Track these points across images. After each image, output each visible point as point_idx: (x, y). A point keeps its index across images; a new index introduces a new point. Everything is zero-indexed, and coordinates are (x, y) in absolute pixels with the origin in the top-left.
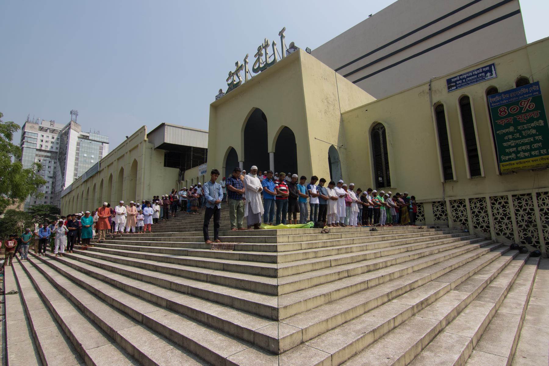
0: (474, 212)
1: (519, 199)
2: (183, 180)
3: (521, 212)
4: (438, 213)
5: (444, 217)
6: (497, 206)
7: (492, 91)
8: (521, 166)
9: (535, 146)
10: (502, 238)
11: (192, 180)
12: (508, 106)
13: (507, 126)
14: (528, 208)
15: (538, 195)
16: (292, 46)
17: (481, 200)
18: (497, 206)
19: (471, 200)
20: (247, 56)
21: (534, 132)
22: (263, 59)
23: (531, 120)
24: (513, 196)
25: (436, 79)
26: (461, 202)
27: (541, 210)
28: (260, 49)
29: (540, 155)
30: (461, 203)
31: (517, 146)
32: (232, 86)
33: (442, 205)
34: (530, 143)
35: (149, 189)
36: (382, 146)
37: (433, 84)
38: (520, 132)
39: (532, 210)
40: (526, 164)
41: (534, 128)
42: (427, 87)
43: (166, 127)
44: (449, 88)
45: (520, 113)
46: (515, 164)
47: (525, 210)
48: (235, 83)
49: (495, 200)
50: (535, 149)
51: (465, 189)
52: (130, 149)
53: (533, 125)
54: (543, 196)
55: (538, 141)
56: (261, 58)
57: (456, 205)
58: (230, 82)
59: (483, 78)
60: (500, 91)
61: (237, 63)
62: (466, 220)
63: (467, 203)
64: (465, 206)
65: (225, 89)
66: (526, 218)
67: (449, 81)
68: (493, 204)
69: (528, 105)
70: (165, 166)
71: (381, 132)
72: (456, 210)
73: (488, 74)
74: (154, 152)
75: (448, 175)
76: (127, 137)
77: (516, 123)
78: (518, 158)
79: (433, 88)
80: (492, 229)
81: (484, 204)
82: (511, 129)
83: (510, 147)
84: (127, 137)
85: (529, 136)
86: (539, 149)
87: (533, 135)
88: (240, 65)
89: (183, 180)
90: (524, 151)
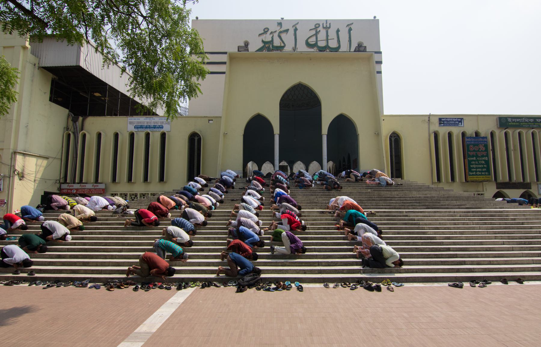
7: (463, 134)
8: (477, 179)
9: (484, 170)
11: (116, 136)
12: (474, 145)
13: (473, 156)
21: (483, 162)
23: (483, 156)
25: (433, 115)
29: (485, 175)
31: (476, 168)
34: (482, 168)
35: (27, 134)
36: (393, 150)
38: (478, 161)
40: (480, 179)
41: (484, 160)
42: (427, 119)
44: (440, 124)
45: (478, 151)
46: (475, 178)
50: (484, 172)
53: (483, 159)
55: (484, 168)
59: (457, 125)
67: (440, 120)
69: (482, 148)
70: (51, 100)
74: (37, 72)
75: (439, 179)
77: (477, 156)
78: (476, 175)
79: (431, 121)
82: (474, 158)
83: (473, 168)
85: (482, 164)
86: (485, 172)
87: (483, 164)
90: (479, 172)
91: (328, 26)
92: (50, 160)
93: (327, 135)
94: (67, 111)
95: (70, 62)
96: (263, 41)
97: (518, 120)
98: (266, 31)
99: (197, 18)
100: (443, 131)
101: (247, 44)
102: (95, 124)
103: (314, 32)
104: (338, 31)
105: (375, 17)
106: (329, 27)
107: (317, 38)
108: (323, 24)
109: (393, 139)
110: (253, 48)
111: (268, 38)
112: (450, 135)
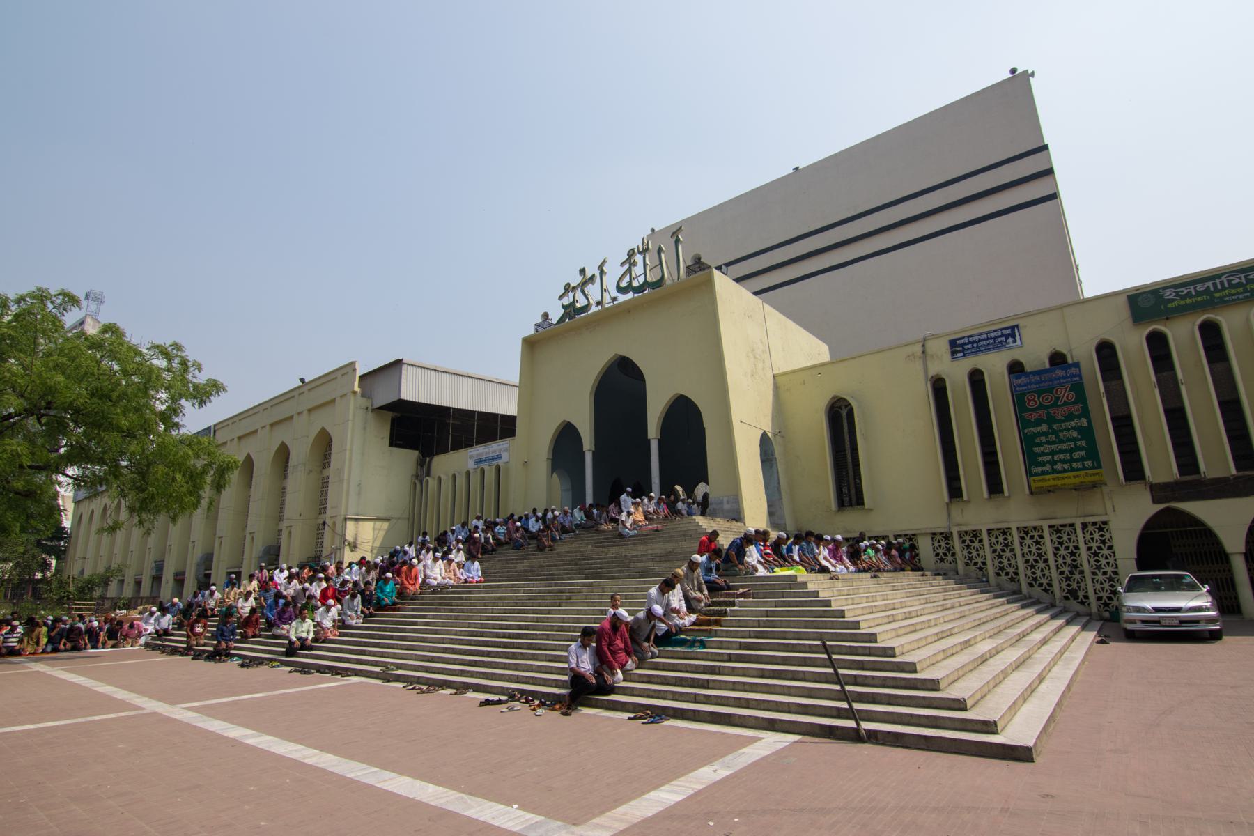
0: (994, 551)
1: (1058, 531)
2: (428, 475)
3: (1062, 552)
4: (941, 552)
5: (949, 558)
6: (1028, 541)
7: (1015, 368)
8: (1059, 483)
9: (1077, 455)
10: (1037, 591)
11: (454, 477)
12: (1039, 393)
13: (1038, 423)
14: (1071, 545)
15: (1084, 526)
17: (1005, 532)
18: (1028, 541)
19: (989, 531)
20: (604, 261)
21: (1075, 434)
22: (638, 270)
23: (1070, 417)
24: (1050, 527)
25: (933, 337)
26: (976, 534)
27: (1089, 549)
28: (631, 254)
29: (1085, 468)
30: (975, 536)
31: (1053, 453)
32: (571, 311)
33: (947, 538)
34: (1071, 451)
35: (359, 494)
36: (847, 437)
37: (929, 344)
38: (1056, 432)
39: (1077, 548)
40: (1066, 481)
41: (1074, 428)
42: (918, 349)
43: (404, 367)
44: (953, 353)
45: (1055, 405)
46: (1051, 480)
47: (1067, 548)
48: (578, 305)
49: (1024, 531)
50: (1077, 460)
51: (980, 514)
52: (310, 406)
53: (1073, 424)
54: (1091, 528)
55: (1080, 449)
57: (967, 538)
58: (566, 301)
59: (1003, 345)
60: (1028, 368)
61: (582, 271)
62: (984, 563)
63: (985, 536)
64: (981, 541)
66: (1069, 560)
67: (953, 343)
68: (1023, 538)
69: (1065, 394)
70: (391, 445)
71: (844, 413)
72: (968, 547)
73: (1010, 340)
74: (370, 415)
75: (955, 491)
76: (302, 380)
77: (1051, 420)
78: (1055, 471)
79: (929, 351)
80: (1022, 577)
81: (1010, 539)
82: (1044, 428)
83: (1043, 454)
84: (302, 380)
85: (1068, 440)
86: (1082, 459)
87: (1074, 440)
88: (588, 275)
89: (428, 475)
90: (1063, 462)
92: (394, 521)
93: (660, 441)
94: (416, 453)
96: (563, 306)
97: (1201, 287)
98: (568, 288)
99: (653, 230)
100: (956, 373)
101: (546, 316)
105: (1013, 71)
112: (976, 379)
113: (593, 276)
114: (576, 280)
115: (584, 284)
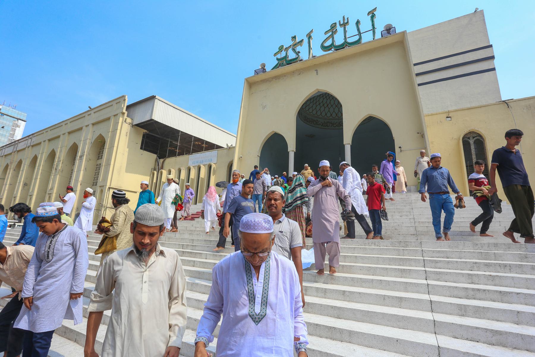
2: (162, 168)
16: (389, 29)
28: (333, 26)
32: (284, 62)
43: (156, 100)
48: (290, 58)
56: (335, 36)
58: (279, 56)
61: (294, 38)
65: (271, 63)
70: (141, 148)
76: (90, 107)
84: (90, 107)
91: (346, 21)
95: (147, 118)
96: (277, 59)
98: (281, 48)
101: (263, 66)
102: (173, 164)
103: (331, 33)
104: (358, 23)
106: (348, 22)
107: (333, 38)
108: (340, 22)
109: (472, 142)
110: (268, 68)
111: (283, 54)
113: (302, 41)
114: (289, 42)
115: (295, 45)
